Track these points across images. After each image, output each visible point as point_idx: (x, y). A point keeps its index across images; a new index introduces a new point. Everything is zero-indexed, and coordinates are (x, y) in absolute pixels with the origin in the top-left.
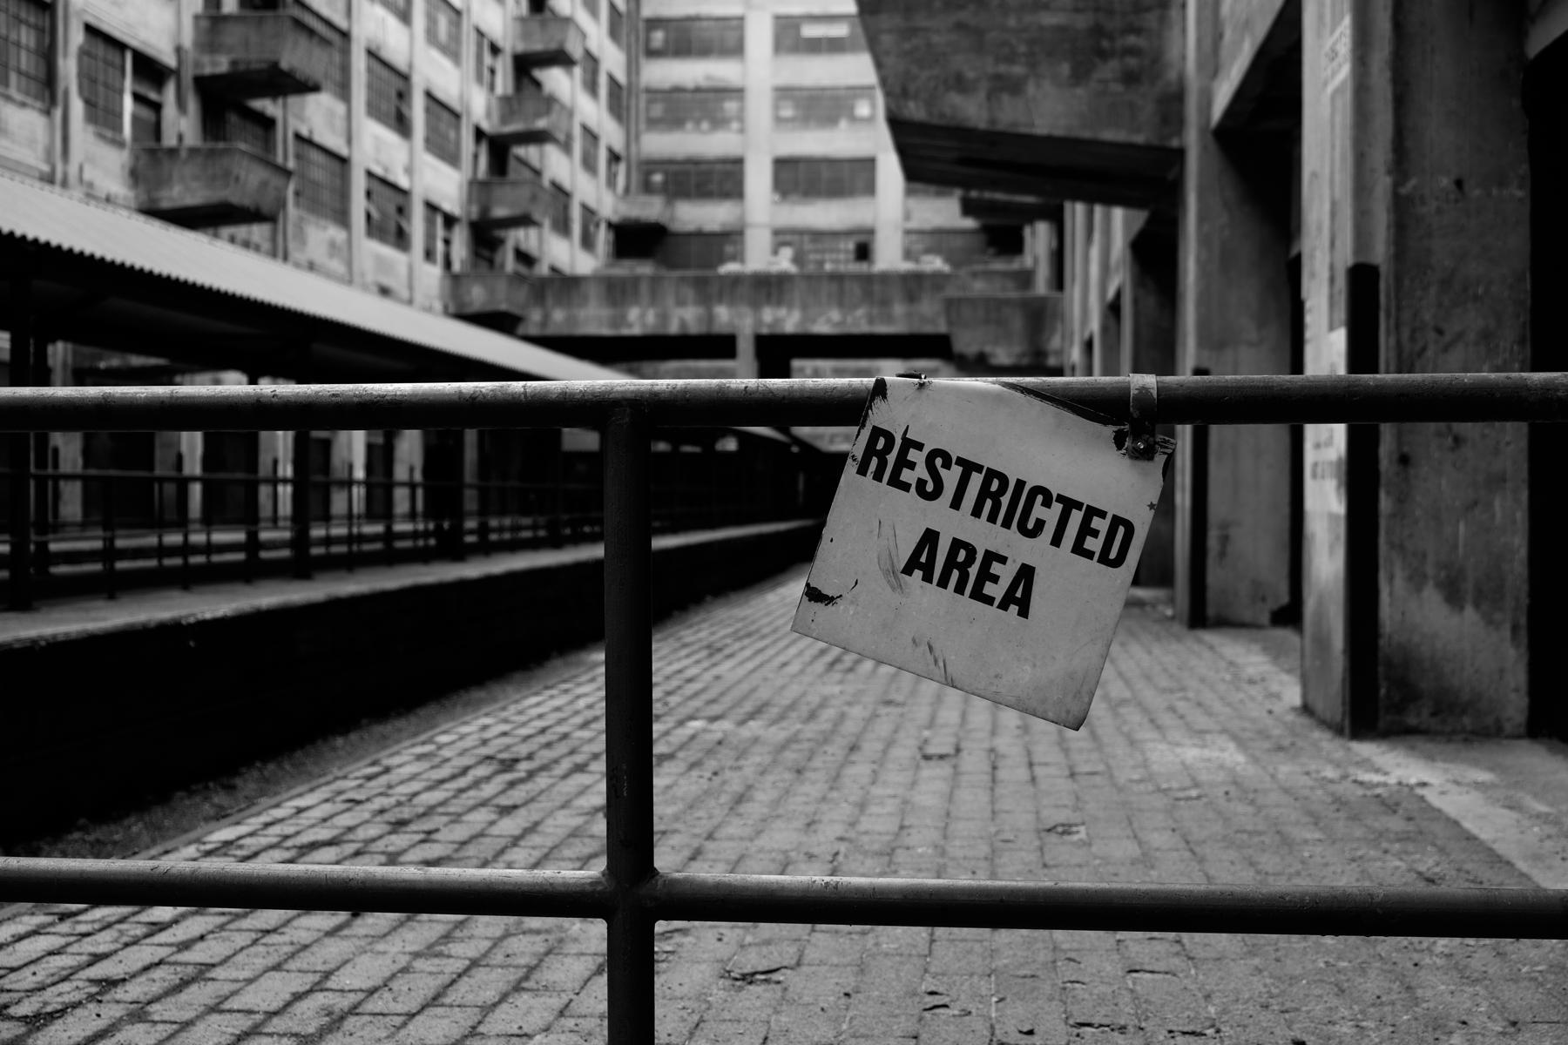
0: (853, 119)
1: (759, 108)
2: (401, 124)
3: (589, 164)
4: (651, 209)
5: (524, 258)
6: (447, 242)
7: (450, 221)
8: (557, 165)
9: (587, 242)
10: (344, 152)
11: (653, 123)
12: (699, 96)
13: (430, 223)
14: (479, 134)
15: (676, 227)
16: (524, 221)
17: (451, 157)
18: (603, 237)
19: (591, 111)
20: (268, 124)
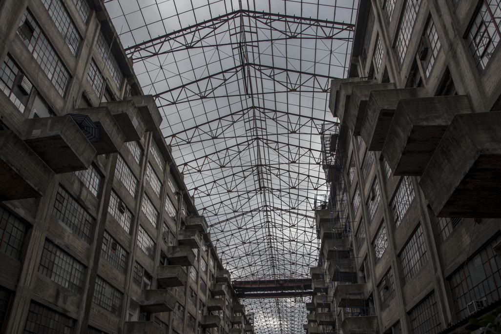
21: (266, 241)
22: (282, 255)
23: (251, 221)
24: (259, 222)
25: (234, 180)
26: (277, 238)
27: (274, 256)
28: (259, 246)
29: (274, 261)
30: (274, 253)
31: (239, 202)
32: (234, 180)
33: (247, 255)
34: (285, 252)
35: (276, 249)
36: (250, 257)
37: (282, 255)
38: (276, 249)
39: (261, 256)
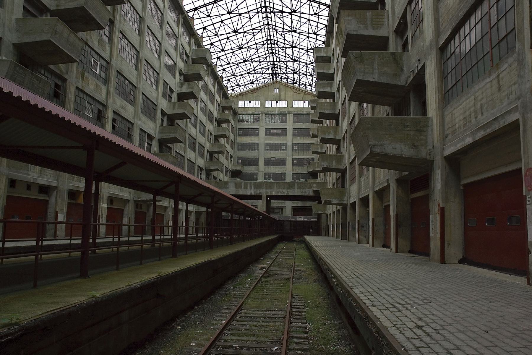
0: (282, 150)
1: (262, 147)
2: (194, 150)
3: (227, 158)
4: (239, 168)
5: (215, 178)
6: (201, 174)
7: (202, 169)
8: (222, 158)
9: (226, 175)
10: (184, 155)
11: (239, 150)
12: (249, 144)
13: (198, 170)
14: (208, 151)
15: (244, 171)
16: (217, 170)
17: (202, 156)
18: (229, 174)
19: (228, 147)
20: (170, 148)
21: (266, 46)
22: (284, 62)
23: (253, 39)
24: (261, 40)
25: (244, 35)
26: (280, 56)
27: (276, 63)
28: (259, 51)
29: (276, 69)
30: (275, 60)
31: (244, 38)
32: (244, 35)
33: (245, 61)
34: (288, 59)
35: (277, 55)
36: (248, 64)
37: (284, 62)
38: (277, 55)
39: (260, 62)
